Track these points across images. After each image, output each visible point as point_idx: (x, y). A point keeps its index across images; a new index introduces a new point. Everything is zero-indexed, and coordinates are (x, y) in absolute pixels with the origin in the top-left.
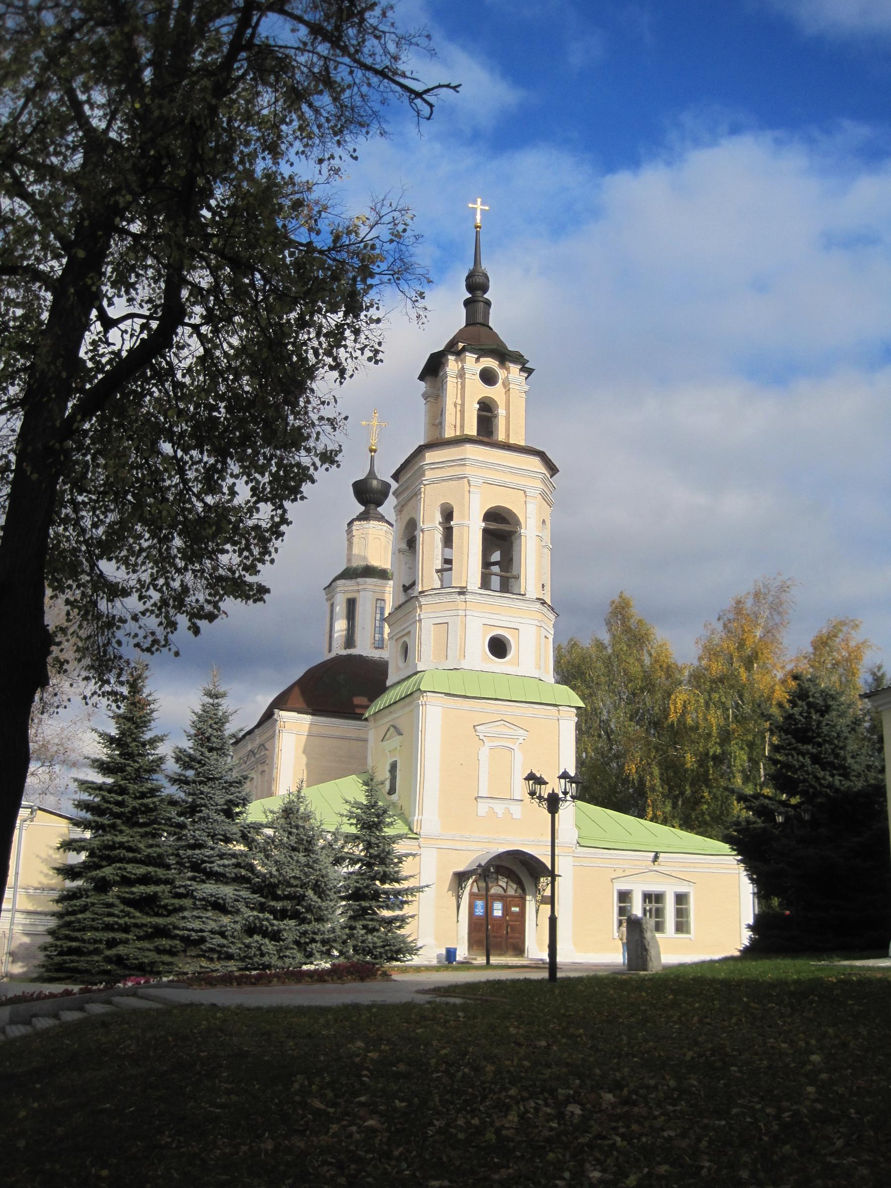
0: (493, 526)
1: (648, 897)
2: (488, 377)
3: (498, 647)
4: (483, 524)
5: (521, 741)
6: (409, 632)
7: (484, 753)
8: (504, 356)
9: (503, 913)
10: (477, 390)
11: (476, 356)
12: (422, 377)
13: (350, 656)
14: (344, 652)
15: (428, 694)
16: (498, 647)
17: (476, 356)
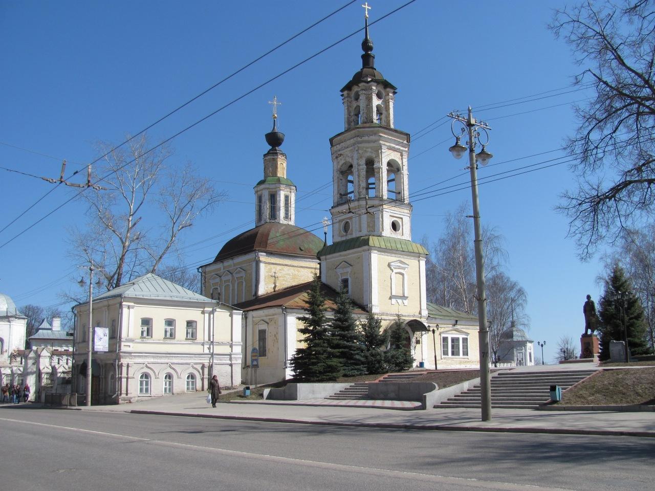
1: (453, 340)
3: (395, 226)
4: (387, 168)
12: (342, 91)
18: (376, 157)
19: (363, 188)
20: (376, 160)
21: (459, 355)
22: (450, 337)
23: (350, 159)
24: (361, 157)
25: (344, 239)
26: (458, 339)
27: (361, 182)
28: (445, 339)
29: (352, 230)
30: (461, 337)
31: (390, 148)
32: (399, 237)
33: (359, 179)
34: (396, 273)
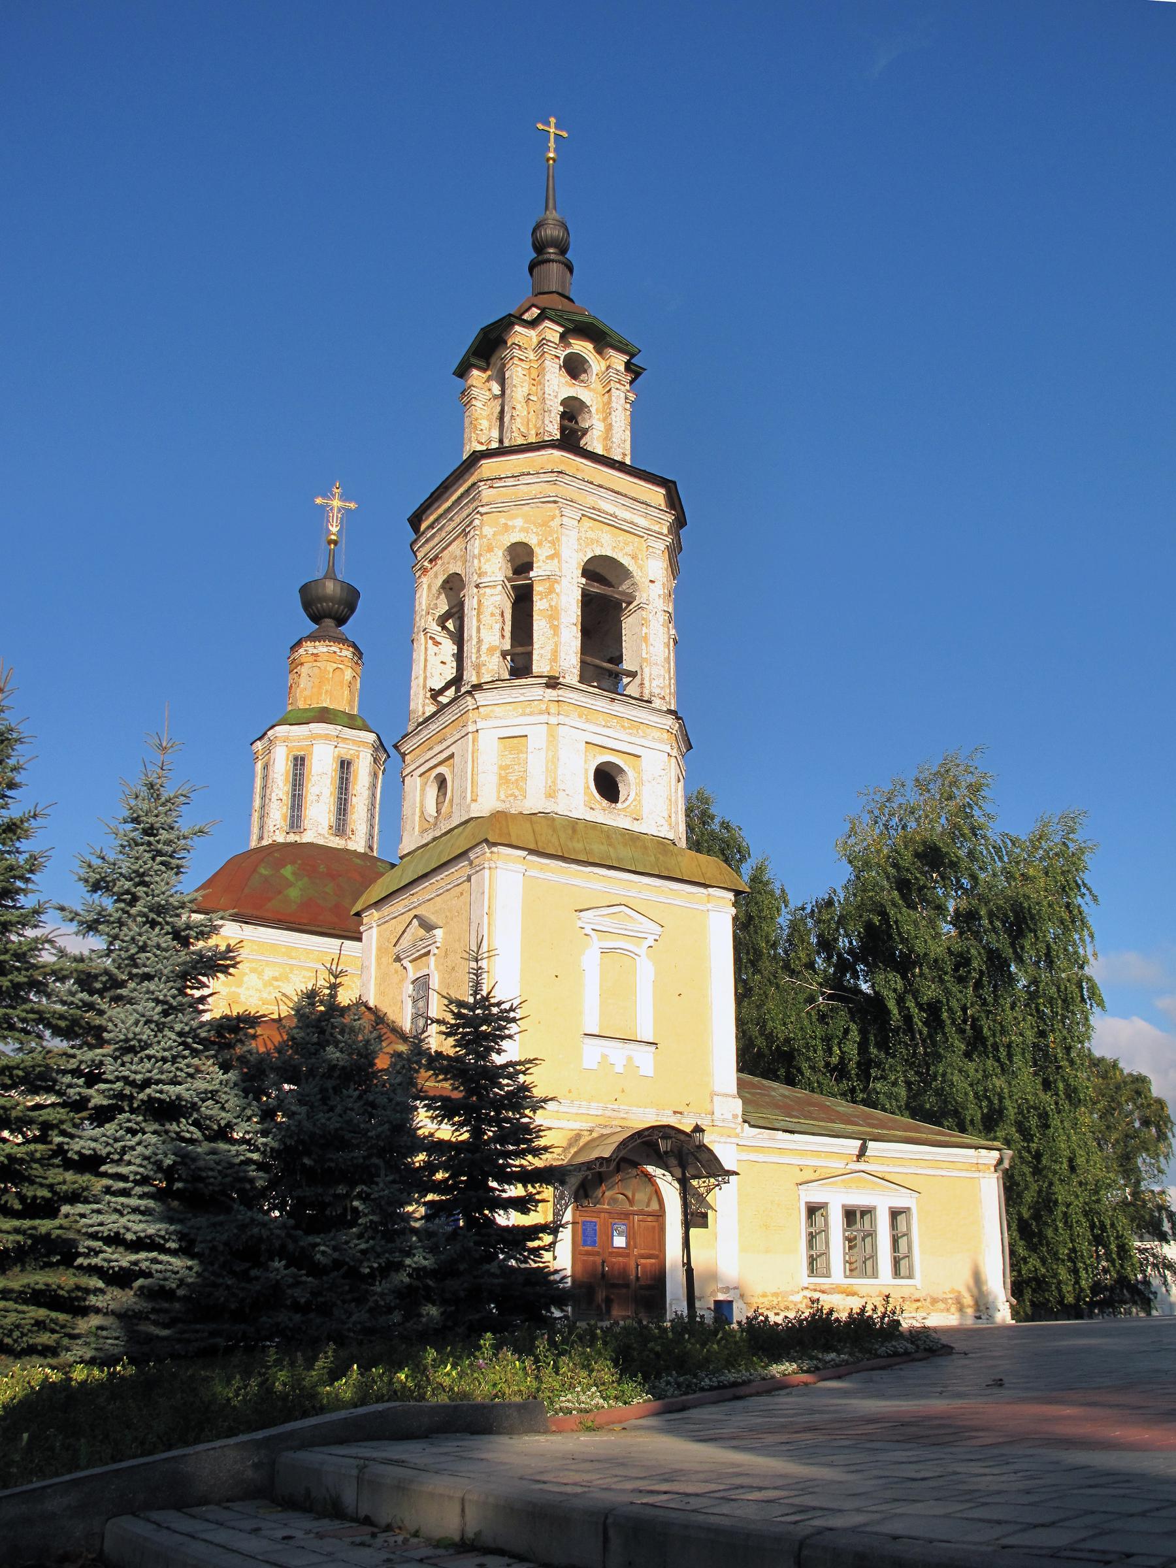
0: (596, 588)
2: (574, 367)
3: (607, 782)
4: (584, 581)
5: (650, 942)
6: (452, 756)
7: (591, 959)
8: (601, 339)
9: (628, 1243)
10: (559, 386)
11: (561, 330)
13: (295, 845)
14: (280, 838)
15: (502, 849)
16: (607, 782)
17: (561, 330)
18: (540, 544)
19: (491, 650)
20: (541, 556)
21: (875, 1275)
22: (836, 1200)
23: (459, 563)
24: (490, 549)
25: (428, 838)
26: (868, 1212)
27: (484, 633)
28: (813, 1210)
29: (452, 800)
30: (882, 1202)
31: (595, 516)
32: (623, 822)
33: (479, 621)
34: (604, 952)
